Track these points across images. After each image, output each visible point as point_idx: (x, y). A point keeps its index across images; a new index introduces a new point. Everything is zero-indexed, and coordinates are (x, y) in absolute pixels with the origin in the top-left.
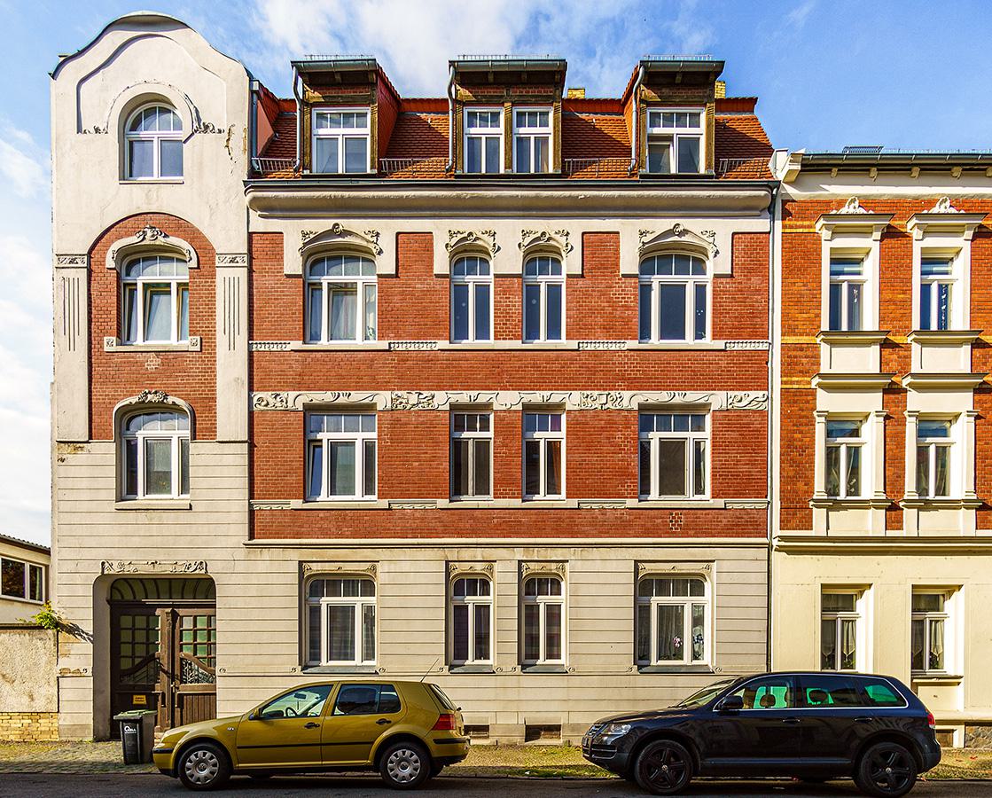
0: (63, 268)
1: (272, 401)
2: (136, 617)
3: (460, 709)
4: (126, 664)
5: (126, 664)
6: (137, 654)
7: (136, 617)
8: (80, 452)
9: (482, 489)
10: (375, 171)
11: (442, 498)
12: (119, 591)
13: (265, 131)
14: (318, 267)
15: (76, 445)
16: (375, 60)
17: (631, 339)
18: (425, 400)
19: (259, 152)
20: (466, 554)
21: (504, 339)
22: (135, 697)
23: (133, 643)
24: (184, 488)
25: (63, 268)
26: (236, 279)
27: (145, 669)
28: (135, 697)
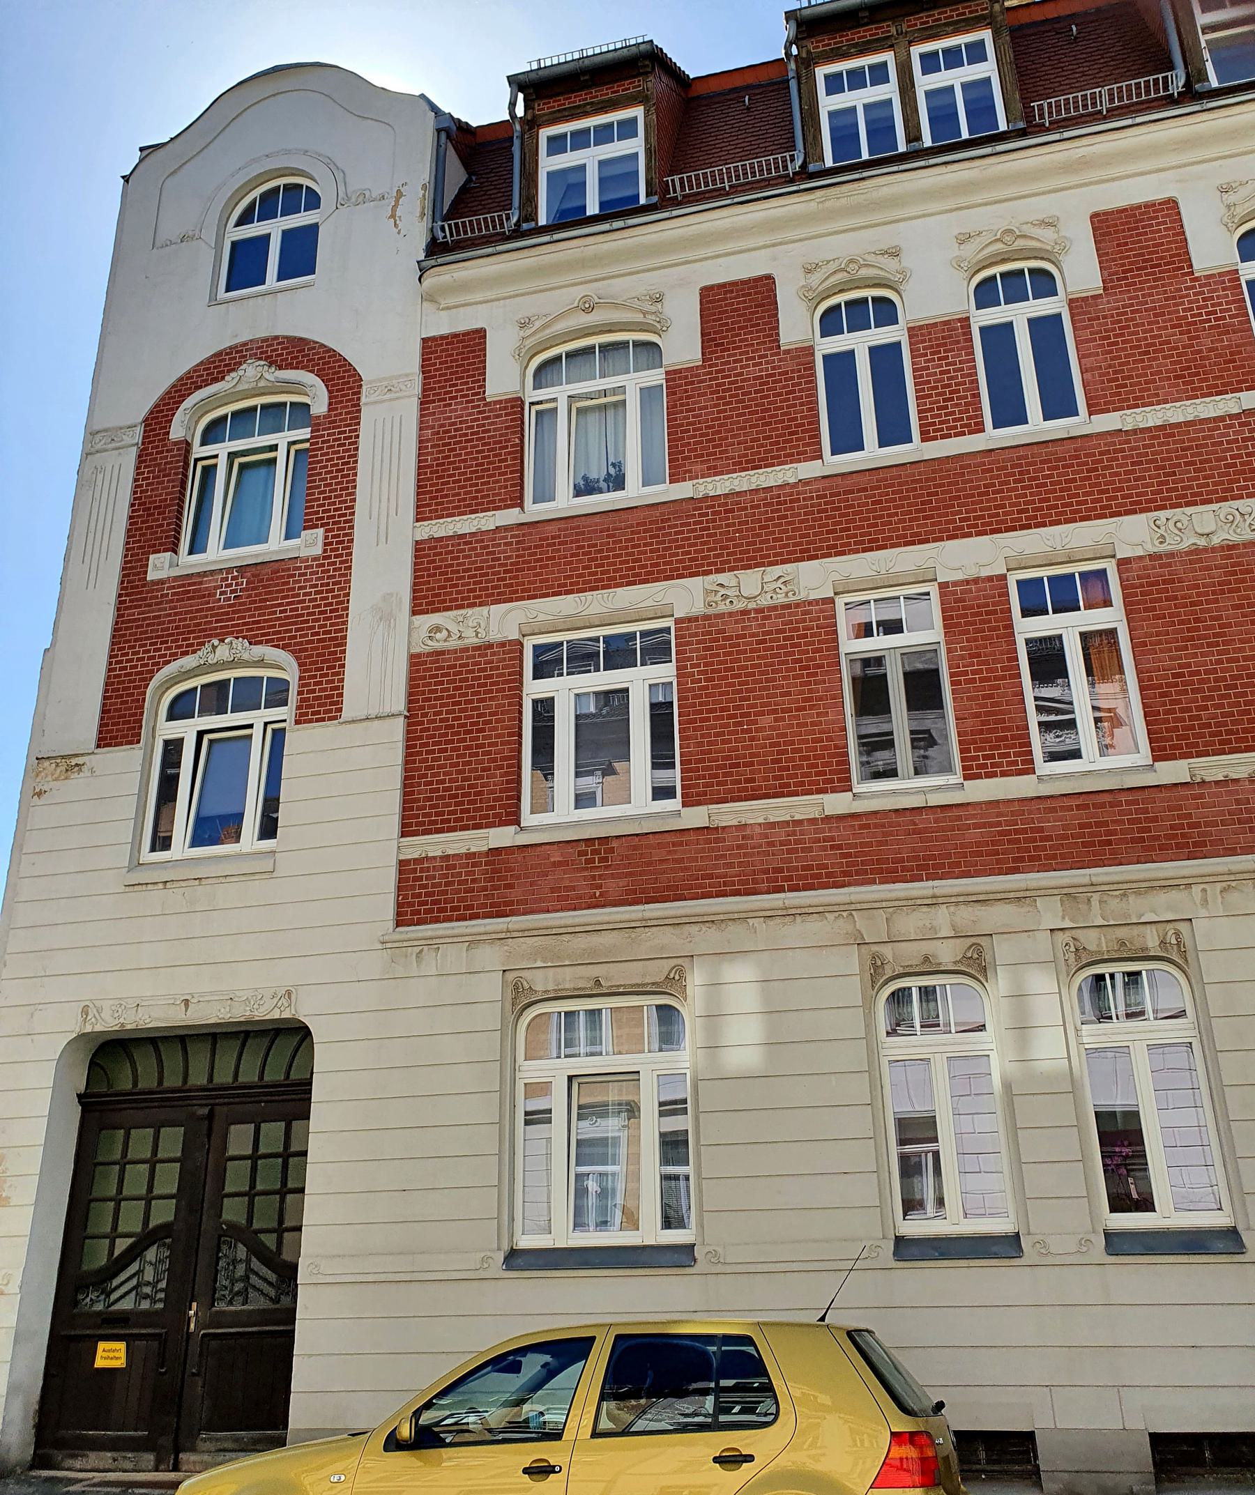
0: (376, 402)
1: (454, 628)
2: (133, 1132)
3: (940, 1406)
4: (97, 1256)
5: (97, 1256)
6: (122, 1228)
7: (133, 1132)
8: (76, 775)
9: (893, 432)
10: (655, 199)
11: (834, 791)
12: (103, 1068)
13: (456, 175)
14: (548, 375)
15: (70, 764)
16: (652, 41)
17: (1248, 389)
18: (779, 584)
19: (445, 212)
20: (910, 923)
21: (943, 437)
22: (102, 1346)
23: (153, 1162)
24: (269, 829)
25: (376, 402)
26: (397, 420)
27: (134, 1268)
28: (102, 1346)
